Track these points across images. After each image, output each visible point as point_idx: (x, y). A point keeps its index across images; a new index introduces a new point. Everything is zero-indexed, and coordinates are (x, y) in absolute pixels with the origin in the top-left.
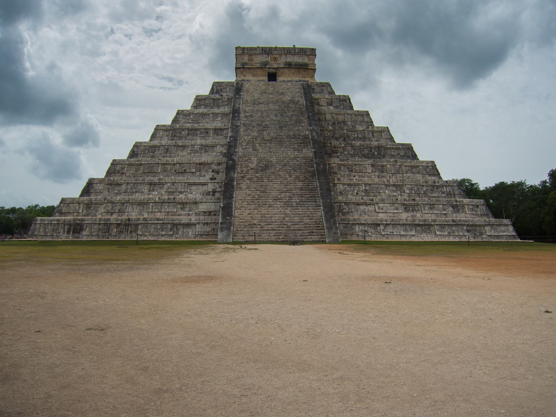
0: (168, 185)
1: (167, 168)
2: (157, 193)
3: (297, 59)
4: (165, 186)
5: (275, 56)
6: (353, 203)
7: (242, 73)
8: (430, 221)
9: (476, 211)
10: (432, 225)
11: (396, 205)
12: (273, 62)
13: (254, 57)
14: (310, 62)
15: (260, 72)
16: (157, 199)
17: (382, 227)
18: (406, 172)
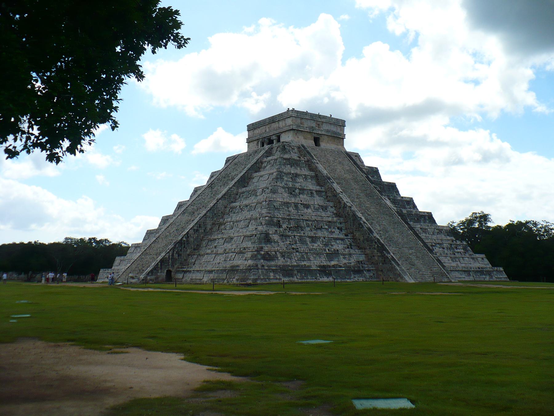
3: (333, 128)
7: (296, 134)
10: (470, 271)
13: (303, 121)
14: (341, 132)
15: (309, 136)
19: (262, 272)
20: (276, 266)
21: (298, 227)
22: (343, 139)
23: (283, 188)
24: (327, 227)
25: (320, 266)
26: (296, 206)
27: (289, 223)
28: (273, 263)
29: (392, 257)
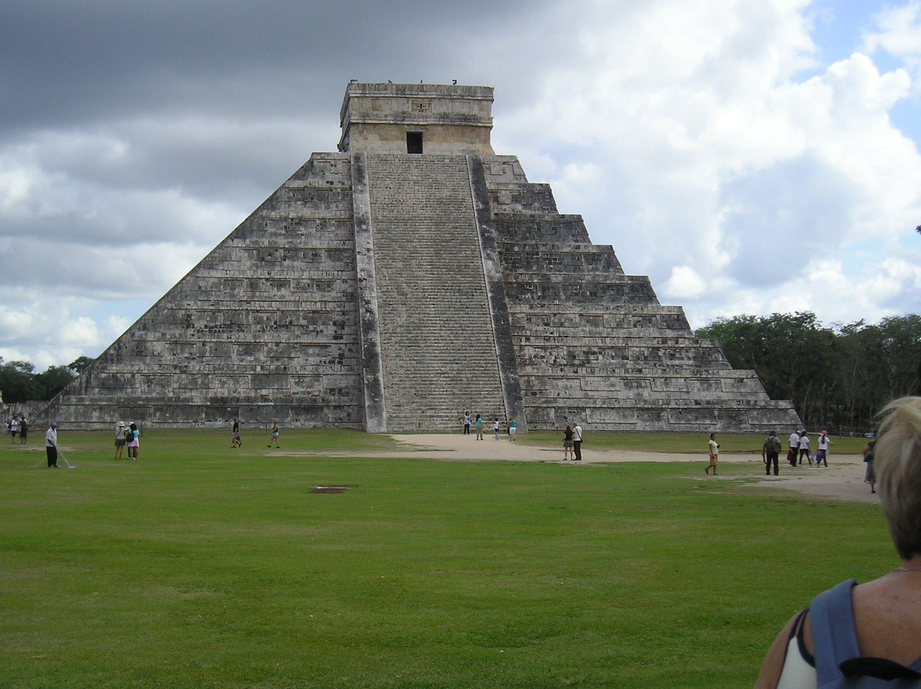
0: (270, 345)
1: (261, 318)
2: (252, 359)
3: (460, 108)
4: (266, 349)
5: (420, 102)
6: (549, 377)
8: (661, 403)
9: (738, 388)
10: (663, 409)
11: (612, 379)
12: (417, 113)
13: (380, 102)
14: (482, 114)
15: (395, 132)
16: (258, 368)
17: (588, 412)
18: (635, 326)
19: (75, 410)
20: (111, 400)
21: (233, 325)
22: (491, 128)
23: (247, 249)
24: (304, 322)
25: (214, 400)
26: (253, 284)
27: (214, 318)
28: (120, 395)
29: (376, 380)
